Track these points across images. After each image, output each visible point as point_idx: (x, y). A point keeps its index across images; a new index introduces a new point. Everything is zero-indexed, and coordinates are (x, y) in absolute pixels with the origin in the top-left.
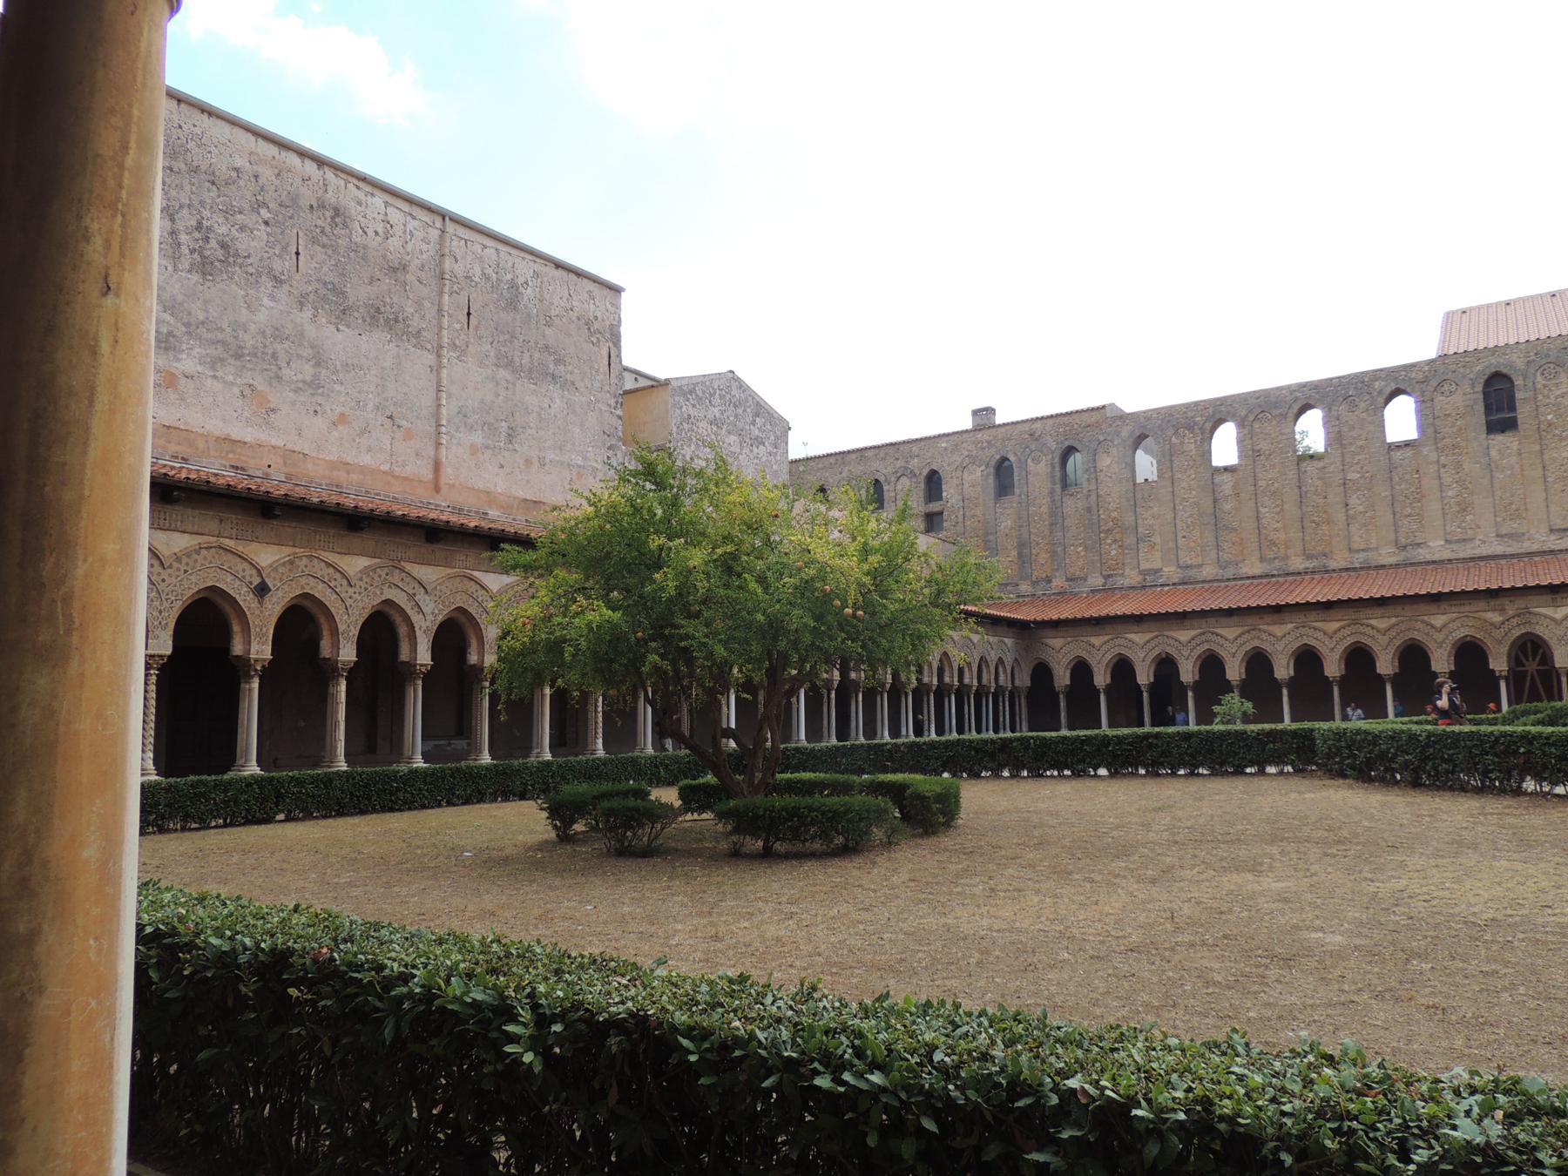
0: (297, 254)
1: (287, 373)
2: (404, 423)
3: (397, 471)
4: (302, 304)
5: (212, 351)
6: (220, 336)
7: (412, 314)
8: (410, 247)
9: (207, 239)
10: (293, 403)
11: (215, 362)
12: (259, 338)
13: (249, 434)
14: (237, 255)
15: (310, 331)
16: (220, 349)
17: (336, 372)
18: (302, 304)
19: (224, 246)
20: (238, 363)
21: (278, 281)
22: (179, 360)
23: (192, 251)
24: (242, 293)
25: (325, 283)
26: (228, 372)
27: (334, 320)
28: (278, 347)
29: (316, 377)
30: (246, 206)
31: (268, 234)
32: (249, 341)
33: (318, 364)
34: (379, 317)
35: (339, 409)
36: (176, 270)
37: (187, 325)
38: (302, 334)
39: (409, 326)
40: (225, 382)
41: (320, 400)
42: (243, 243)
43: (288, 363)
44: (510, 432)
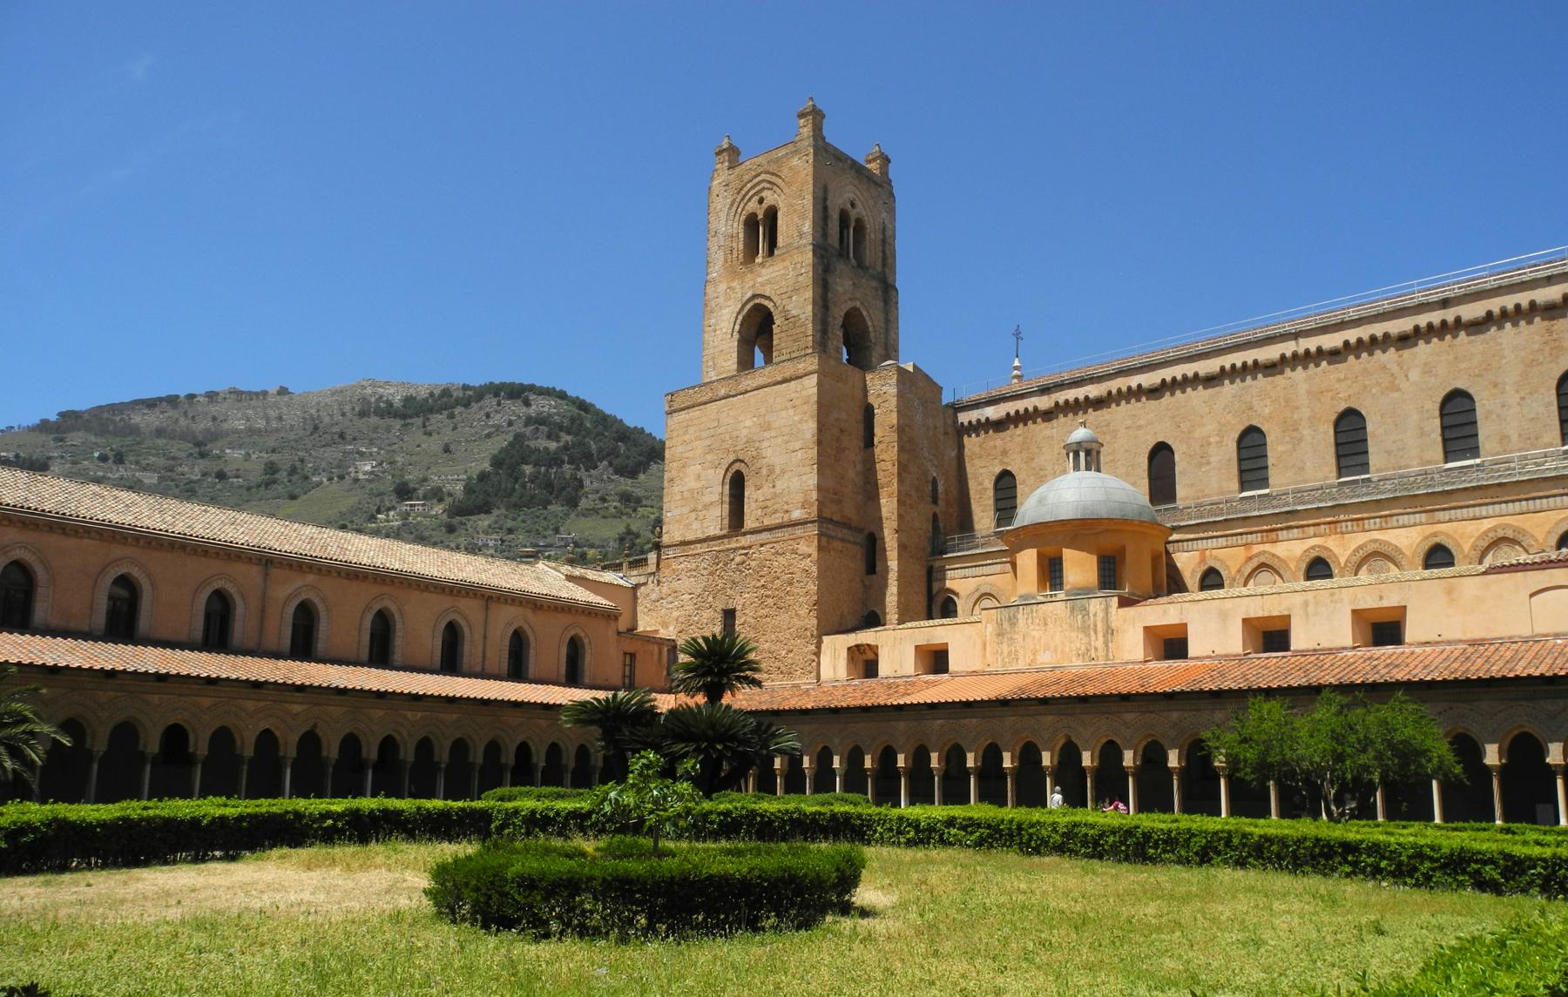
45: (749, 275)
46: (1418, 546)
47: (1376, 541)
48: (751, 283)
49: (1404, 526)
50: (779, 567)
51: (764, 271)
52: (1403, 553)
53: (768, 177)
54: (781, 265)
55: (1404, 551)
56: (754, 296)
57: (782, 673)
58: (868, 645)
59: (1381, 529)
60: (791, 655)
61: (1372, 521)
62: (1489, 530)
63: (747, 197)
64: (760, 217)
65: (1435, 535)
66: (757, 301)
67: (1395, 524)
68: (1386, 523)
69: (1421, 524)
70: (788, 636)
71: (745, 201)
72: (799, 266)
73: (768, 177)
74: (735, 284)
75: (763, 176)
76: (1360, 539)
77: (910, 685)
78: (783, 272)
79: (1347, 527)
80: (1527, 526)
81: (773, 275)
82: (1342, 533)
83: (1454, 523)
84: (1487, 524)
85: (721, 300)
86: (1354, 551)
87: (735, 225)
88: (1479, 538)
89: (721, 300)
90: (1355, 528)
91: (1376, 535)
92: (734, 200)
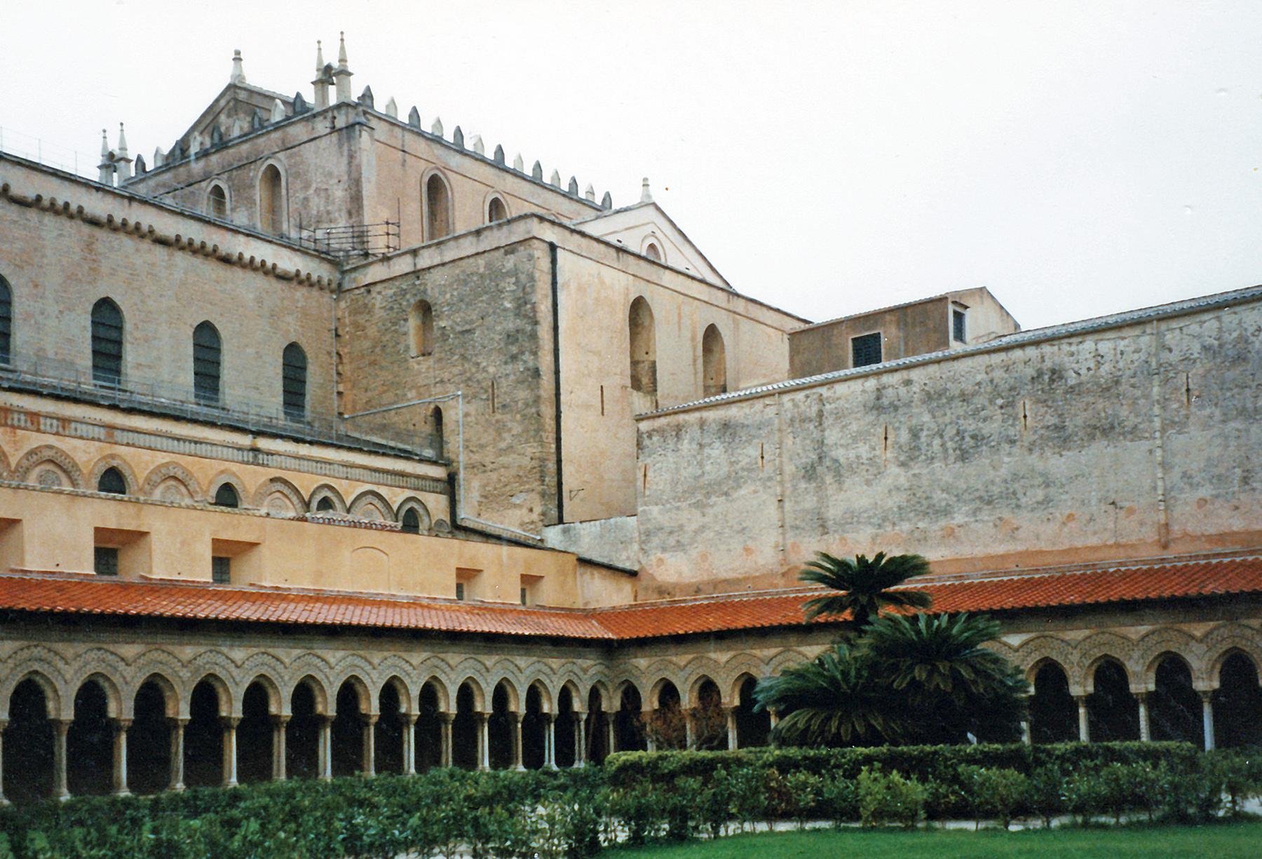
0: (1025, 417)
1: (1023, 500)
2: (1126, 504)
3: (1123, 541)
4: (1030, 450)
5: (973, 506)
6: (977, 494)
7: (1128, 417)
8: (1121, 365)
9: (963, 438)
10: (1030, 520)
11: (975, 512)
12: (1003, 485)
13: (1001, 549)
14: (983, 438)
15: (1040, 466)
16: (978, 502)
17: (1063, 485)
18: (1030, 450)
19: (973, 437)
20: (990, 507)
21: (1013, 442)
22: (953, 519)
23: (954, 450)
24: (988, 461)
25: (1048, 427)
26: (985, 515)
27: (1057, 450)
28: (1016, 485)
29: (1046, 496)
30: (987, 403)
31: (1003, 414)
32: (996, 490)
33: (1048, 486)
34: (1106, 430)
35: (1069, 511)
36: (946, 465)
37: (957, 496)
38: (1033, 470)
39: (1124, 427)
40: (983, 521)
41: (1051, 510)
42: (987, 429)
43: (1025, 494)
44: (1245, 474)
46: (96, 464)
47: (50, 447)
49: (81, 438)
52: (80, 470)
55: (81, 467)
59: (57, 434)
61: (49, 421)
62: (159, 467)
65: (113, 456)
67: (73, 433)
68: (64, 428)
69: (99, 440)
76: (35, 440)
77: (83, 583)
79: (19, 420)
80: (194, 470)
82: (13, 426)
83: (132, 449)
84: (162, 458)
86: (27, 453)
88: (151, 472)
90: (29, 424)
91: (51, 440)
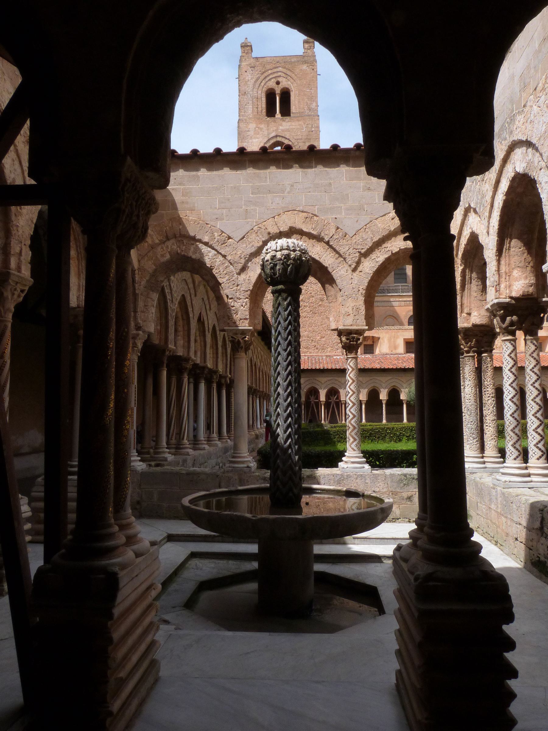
45: (273, 123)
48: (275, 128)
50: (313, 291)
51: (284, 123)
53: (284, 70)
54: (297, 123)
56: (276, 136)
57: (317, 349)
58: (373, 337)
60: (324, 339)
63: (268, 78)
64: (278, 91)
66: (279, 139)
70: (322, 329)
71: (267, 80)
72: (310, 126)
73: (284, 70)
74: (262, 126)
75: (280, 69)
78: (299, 127)
81: (291, 127)
85: (251, 133)
87: (260, 92)
89: (251, 133)
92: (259, 77)
